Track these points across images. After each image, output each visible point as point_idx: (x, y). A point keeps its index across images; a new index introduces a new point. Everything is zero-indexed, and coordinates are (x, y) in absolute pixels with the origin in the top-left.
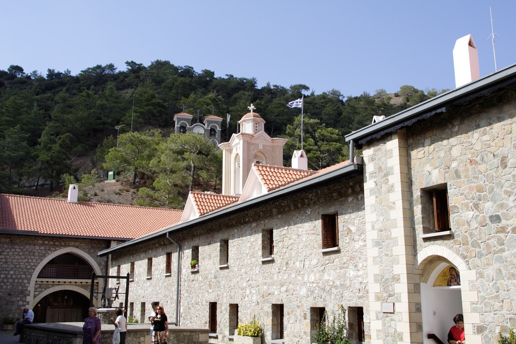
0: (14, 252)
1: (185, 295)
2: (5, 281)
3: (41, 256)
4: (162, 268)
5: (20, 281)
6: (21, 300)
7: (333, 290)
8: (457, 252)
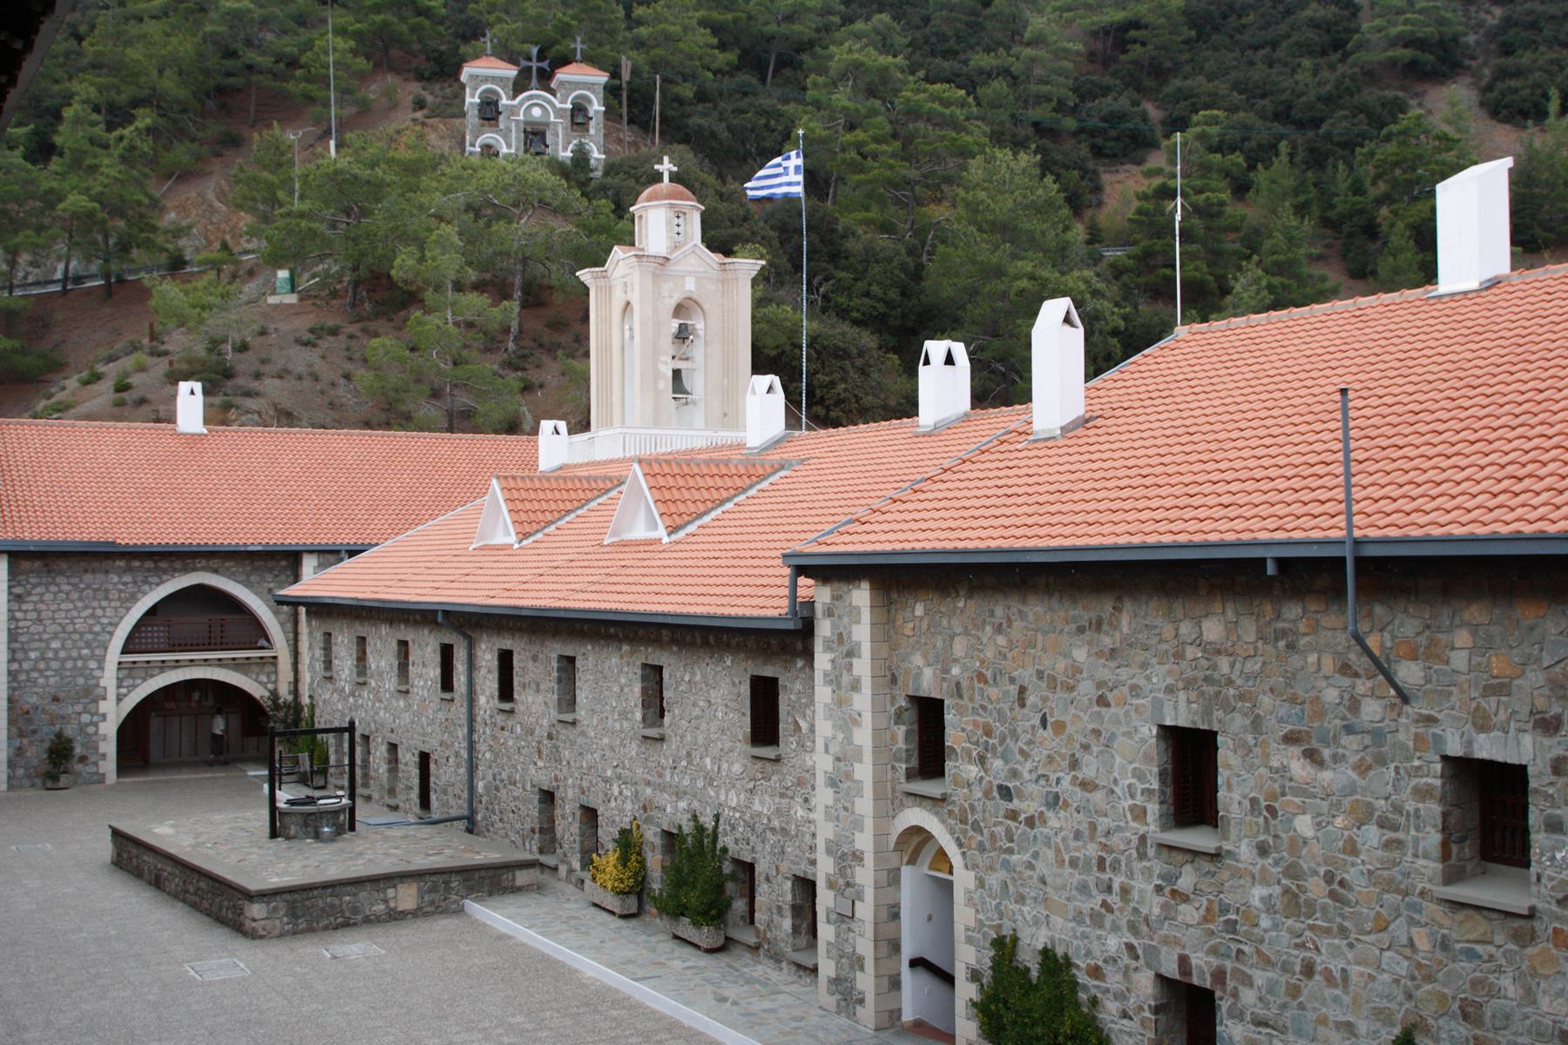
1: (488, 755)
2: (42, 665)
3: (127, 600)
4: (432, 675)
6: (85, 711)
7: (769, 834)
8: (952, 832)
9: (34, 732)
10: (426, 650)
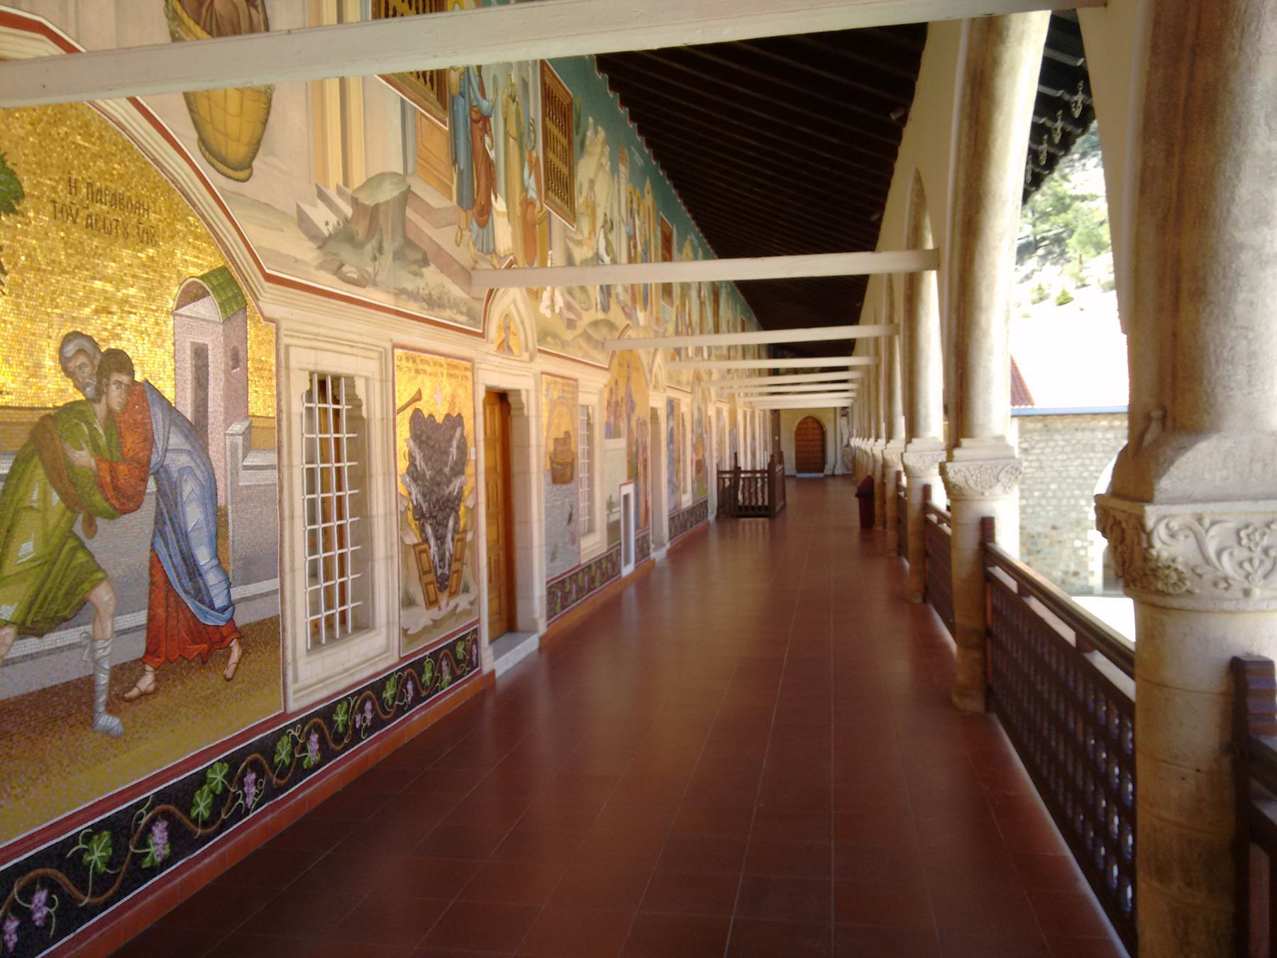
0: (1053, 448)
2: (1043, 502)
5: (1072, 502)
6: (1078, 538)
9: (1038, 552)
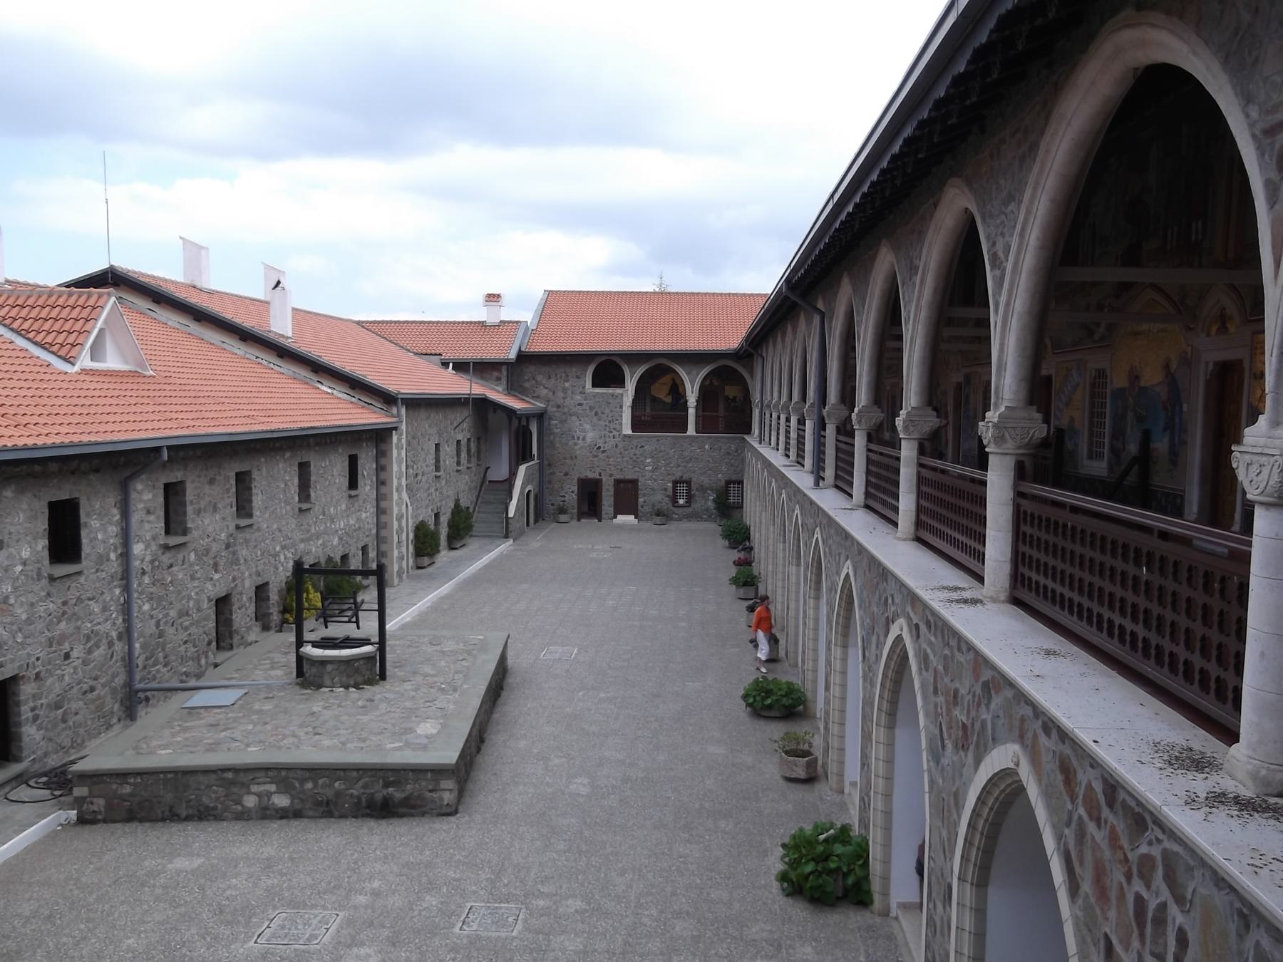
10: (147, 496)
